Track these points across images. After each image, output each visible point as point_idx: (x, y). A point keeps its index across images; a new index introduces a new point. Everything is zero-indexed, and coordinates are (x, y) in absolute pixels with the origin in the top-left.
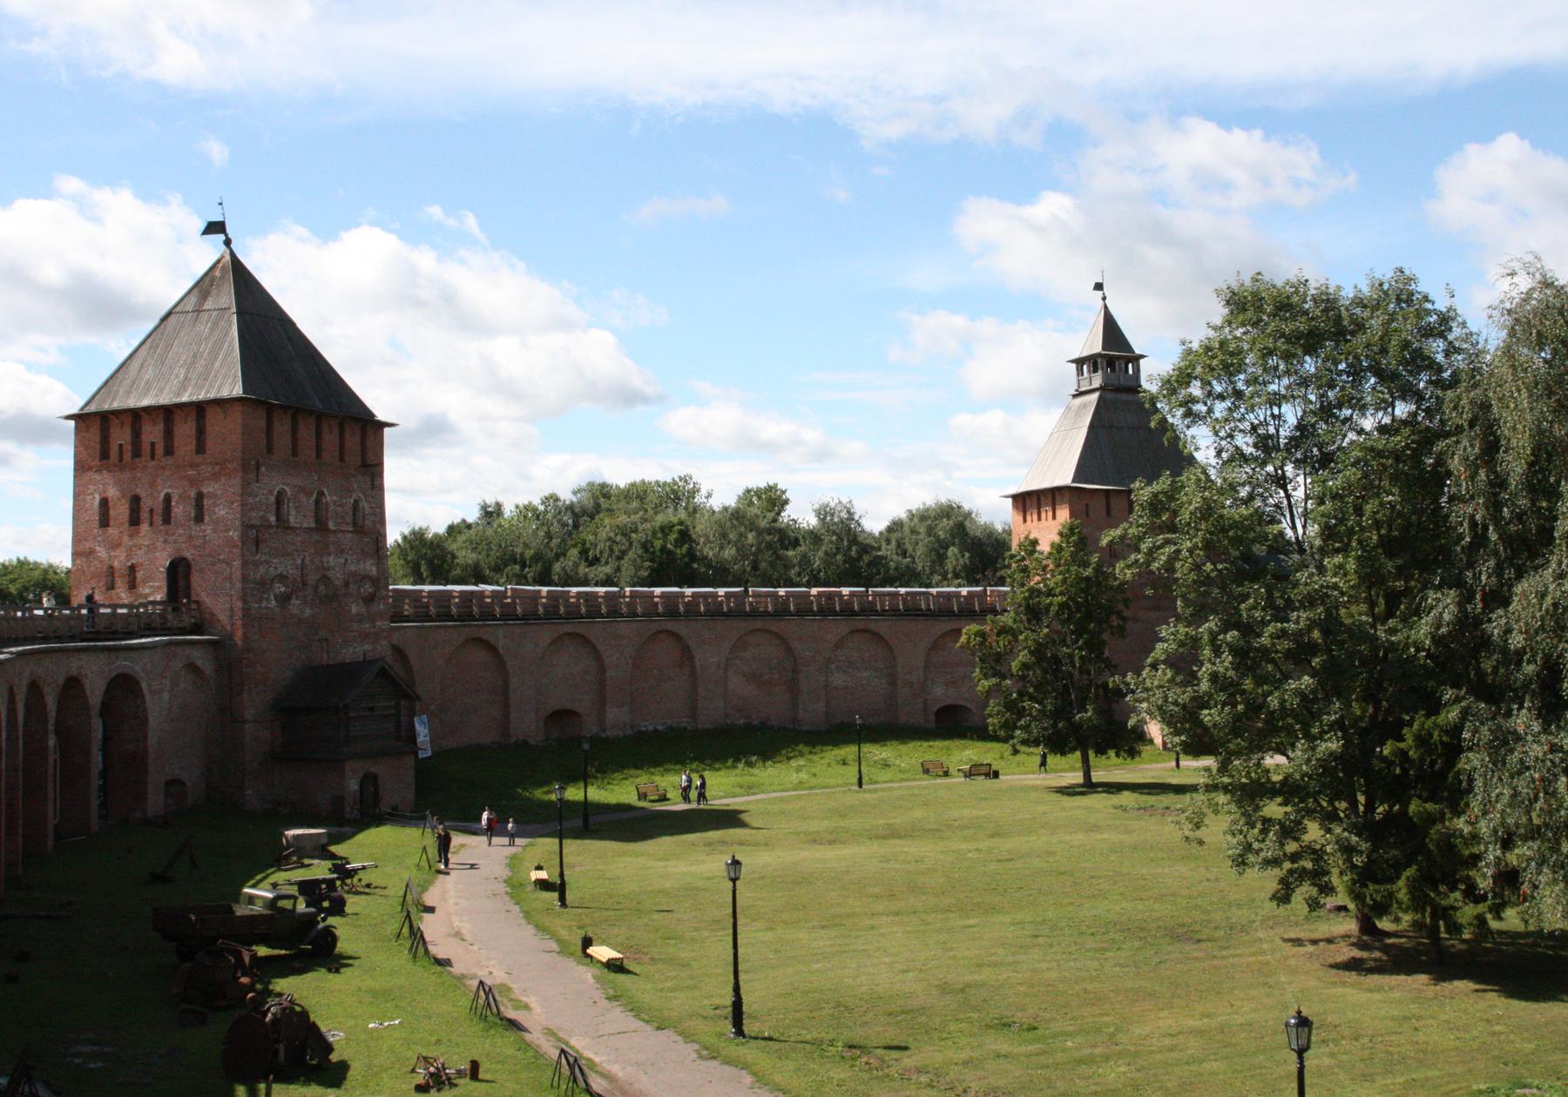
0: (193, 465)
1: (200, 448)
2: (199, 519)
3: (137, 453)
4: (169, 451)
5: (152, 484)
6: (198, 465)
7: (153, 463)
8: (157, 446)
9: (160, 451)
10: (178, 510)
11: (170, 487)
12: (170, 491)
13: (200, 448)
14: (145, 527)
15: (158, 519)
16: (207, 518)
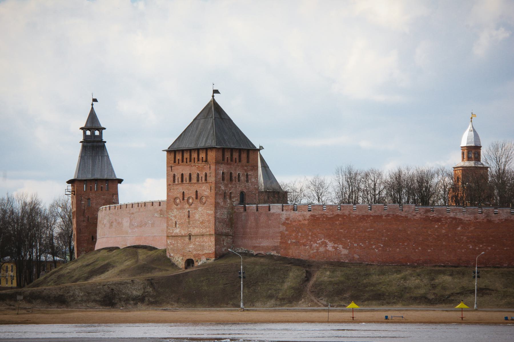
0: (246, 166)
1: (248, 161)
2: (247, 181)
3: (232, 160)
4: (240, 161)
5: (235, 170)
6: (247, 166)
7: (236, 164)
8: (237, 159)
9: (238, 161)
10: (242, 178)
11: (240, 171)
12: (240, 172)
13: (248, 161)
14: (234, 182)
15: (237, 180)
16: (249, 181)
